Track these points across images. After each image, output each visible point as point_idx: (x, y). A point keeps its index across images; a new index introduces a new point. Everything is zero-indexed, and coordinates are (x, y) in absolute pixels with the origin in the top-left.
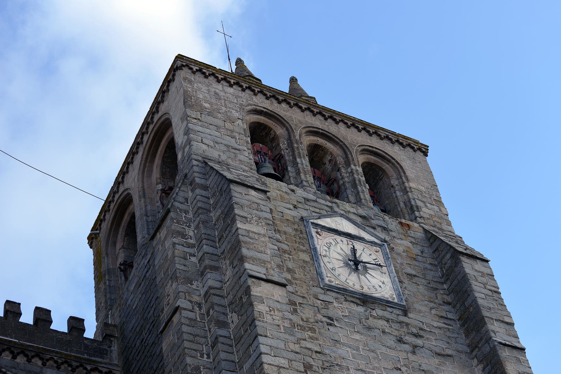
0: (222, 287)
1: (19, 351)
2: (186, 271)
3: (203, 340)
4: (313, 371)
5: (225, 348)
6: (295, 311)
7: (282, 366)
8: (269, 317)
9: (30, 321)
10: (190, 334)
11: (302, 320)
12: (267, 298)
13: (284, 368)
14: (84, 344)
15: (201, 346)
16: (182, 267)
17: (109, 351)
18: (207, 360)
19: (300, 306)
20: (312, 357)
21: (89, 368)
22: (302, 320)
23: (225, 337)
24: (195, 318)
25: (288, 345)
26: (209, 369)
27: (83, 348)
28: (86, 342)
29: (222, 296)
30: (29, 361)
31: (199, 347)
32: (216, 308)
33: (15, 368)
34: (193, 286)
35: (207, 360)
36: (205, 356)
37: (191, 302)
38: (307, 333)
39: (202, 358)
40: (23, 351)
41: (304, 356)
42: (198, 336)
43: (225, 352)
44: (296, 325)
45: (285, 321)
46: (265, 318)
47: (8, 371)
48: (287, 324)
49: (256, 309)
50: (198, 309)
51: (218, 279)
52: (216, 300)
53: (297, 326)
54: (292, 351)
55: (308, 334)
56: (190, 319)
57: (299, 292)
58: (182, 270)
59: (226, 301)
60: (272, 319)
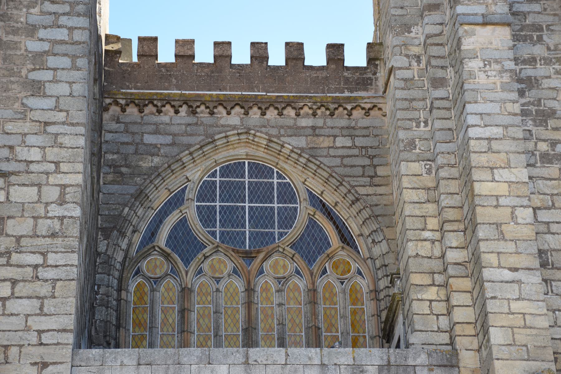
0: (443, 31)
1: (267, 105)
2: (403, 15)
3: (420, 104)
4: (555, 118)
5: (443, 113)
6: (540, 39)
7: (495, 137)
8: (482, 75)
9: (281, 62)
10: (406, 99)
11: (549, 49)
12: (483, 48)
13: (496, 139)
14: (344, 77)
15: (417, 112)
16: (399, 12)
17: (374, 79)
18: (424, 129)
19: (548, 29)
20: (557, 99)
21: (349, 107)
22: (549, 49)
23: (442, 99)
24: (412, 77)
25: (505, 108)
26: (426, 139)
27: (342, 84)
28: (346, 74)
29: (441, 45)
30: (280, 114)
31: (415, 114)
32: (434, 62)
33: (265, 127)
34: (411, 34)
35: (424, 129)
36: (422, 124)
37: (407, 56)
38: (554, 66)
39: (418, 128)
40: (272, 103)
41: (546, 101)
42: (414, 99)
43: (440, 119)
44: (538, 59)
45: (504, 75)
46: (477, 78)
47: (258, 131)
48: (506, 78)
49: (466, 68)
50: (416, 64)
51: (438, 22)
52: (434, 51)
53: (540, 60)
54: (510, 114)
55: (554, 68)
56: (405, 80)
57: (548, 10)
58: (398, 15)
59: (446, 49)
60: (486, 77)
